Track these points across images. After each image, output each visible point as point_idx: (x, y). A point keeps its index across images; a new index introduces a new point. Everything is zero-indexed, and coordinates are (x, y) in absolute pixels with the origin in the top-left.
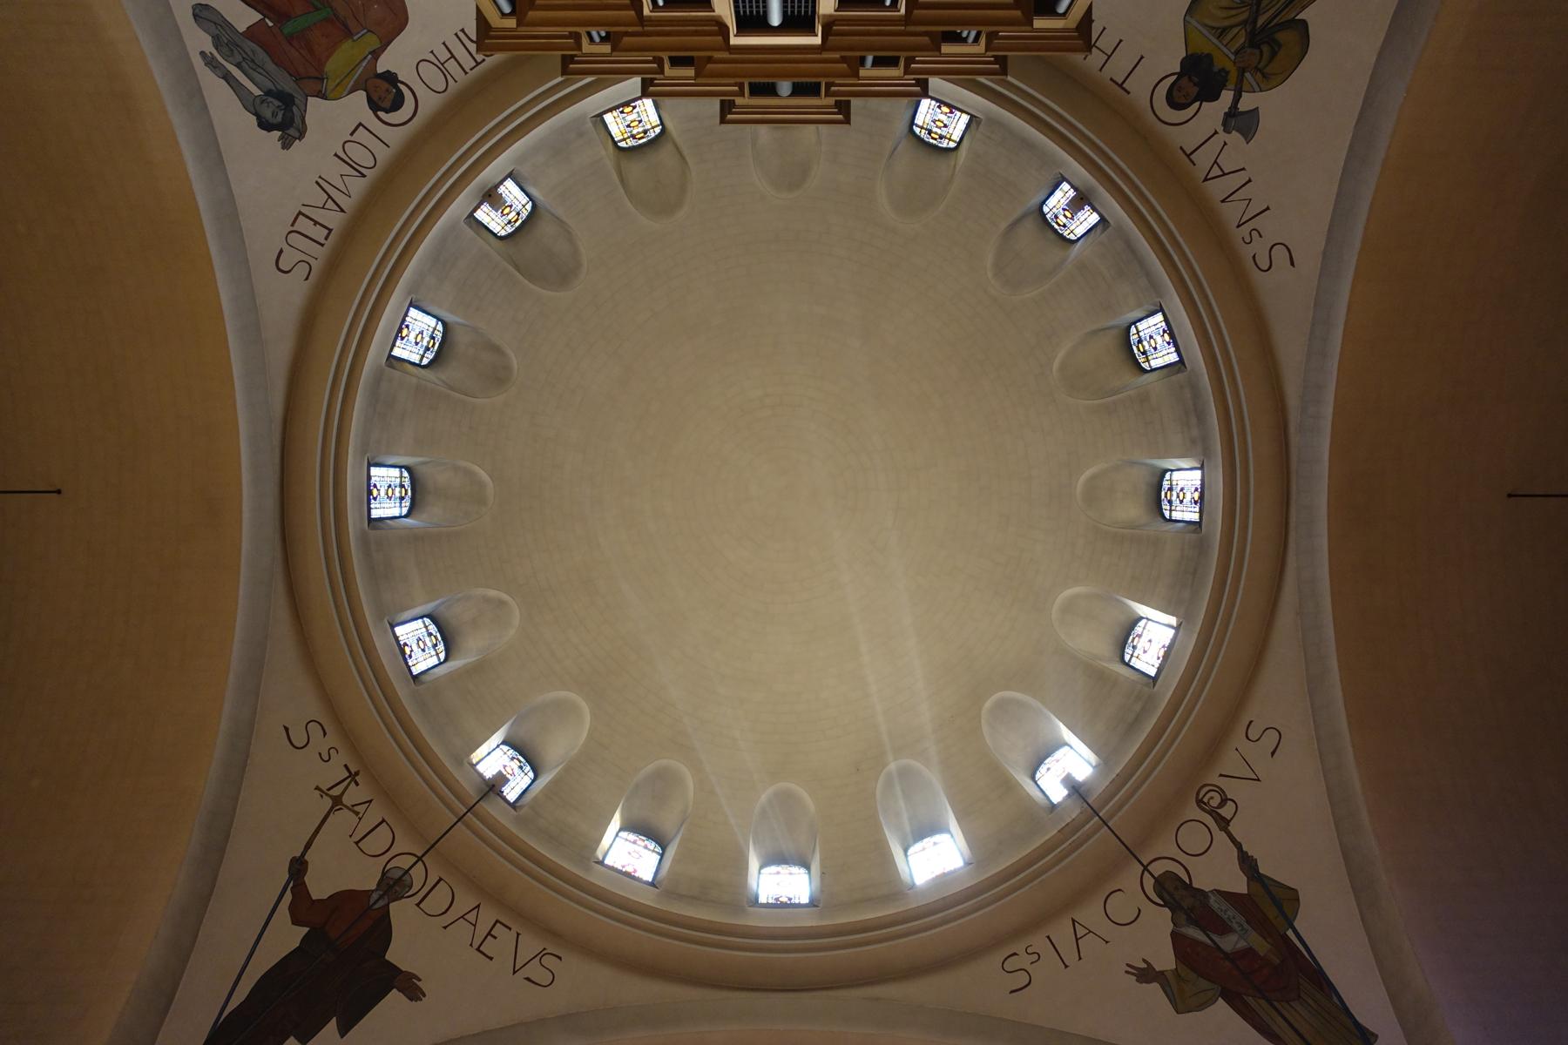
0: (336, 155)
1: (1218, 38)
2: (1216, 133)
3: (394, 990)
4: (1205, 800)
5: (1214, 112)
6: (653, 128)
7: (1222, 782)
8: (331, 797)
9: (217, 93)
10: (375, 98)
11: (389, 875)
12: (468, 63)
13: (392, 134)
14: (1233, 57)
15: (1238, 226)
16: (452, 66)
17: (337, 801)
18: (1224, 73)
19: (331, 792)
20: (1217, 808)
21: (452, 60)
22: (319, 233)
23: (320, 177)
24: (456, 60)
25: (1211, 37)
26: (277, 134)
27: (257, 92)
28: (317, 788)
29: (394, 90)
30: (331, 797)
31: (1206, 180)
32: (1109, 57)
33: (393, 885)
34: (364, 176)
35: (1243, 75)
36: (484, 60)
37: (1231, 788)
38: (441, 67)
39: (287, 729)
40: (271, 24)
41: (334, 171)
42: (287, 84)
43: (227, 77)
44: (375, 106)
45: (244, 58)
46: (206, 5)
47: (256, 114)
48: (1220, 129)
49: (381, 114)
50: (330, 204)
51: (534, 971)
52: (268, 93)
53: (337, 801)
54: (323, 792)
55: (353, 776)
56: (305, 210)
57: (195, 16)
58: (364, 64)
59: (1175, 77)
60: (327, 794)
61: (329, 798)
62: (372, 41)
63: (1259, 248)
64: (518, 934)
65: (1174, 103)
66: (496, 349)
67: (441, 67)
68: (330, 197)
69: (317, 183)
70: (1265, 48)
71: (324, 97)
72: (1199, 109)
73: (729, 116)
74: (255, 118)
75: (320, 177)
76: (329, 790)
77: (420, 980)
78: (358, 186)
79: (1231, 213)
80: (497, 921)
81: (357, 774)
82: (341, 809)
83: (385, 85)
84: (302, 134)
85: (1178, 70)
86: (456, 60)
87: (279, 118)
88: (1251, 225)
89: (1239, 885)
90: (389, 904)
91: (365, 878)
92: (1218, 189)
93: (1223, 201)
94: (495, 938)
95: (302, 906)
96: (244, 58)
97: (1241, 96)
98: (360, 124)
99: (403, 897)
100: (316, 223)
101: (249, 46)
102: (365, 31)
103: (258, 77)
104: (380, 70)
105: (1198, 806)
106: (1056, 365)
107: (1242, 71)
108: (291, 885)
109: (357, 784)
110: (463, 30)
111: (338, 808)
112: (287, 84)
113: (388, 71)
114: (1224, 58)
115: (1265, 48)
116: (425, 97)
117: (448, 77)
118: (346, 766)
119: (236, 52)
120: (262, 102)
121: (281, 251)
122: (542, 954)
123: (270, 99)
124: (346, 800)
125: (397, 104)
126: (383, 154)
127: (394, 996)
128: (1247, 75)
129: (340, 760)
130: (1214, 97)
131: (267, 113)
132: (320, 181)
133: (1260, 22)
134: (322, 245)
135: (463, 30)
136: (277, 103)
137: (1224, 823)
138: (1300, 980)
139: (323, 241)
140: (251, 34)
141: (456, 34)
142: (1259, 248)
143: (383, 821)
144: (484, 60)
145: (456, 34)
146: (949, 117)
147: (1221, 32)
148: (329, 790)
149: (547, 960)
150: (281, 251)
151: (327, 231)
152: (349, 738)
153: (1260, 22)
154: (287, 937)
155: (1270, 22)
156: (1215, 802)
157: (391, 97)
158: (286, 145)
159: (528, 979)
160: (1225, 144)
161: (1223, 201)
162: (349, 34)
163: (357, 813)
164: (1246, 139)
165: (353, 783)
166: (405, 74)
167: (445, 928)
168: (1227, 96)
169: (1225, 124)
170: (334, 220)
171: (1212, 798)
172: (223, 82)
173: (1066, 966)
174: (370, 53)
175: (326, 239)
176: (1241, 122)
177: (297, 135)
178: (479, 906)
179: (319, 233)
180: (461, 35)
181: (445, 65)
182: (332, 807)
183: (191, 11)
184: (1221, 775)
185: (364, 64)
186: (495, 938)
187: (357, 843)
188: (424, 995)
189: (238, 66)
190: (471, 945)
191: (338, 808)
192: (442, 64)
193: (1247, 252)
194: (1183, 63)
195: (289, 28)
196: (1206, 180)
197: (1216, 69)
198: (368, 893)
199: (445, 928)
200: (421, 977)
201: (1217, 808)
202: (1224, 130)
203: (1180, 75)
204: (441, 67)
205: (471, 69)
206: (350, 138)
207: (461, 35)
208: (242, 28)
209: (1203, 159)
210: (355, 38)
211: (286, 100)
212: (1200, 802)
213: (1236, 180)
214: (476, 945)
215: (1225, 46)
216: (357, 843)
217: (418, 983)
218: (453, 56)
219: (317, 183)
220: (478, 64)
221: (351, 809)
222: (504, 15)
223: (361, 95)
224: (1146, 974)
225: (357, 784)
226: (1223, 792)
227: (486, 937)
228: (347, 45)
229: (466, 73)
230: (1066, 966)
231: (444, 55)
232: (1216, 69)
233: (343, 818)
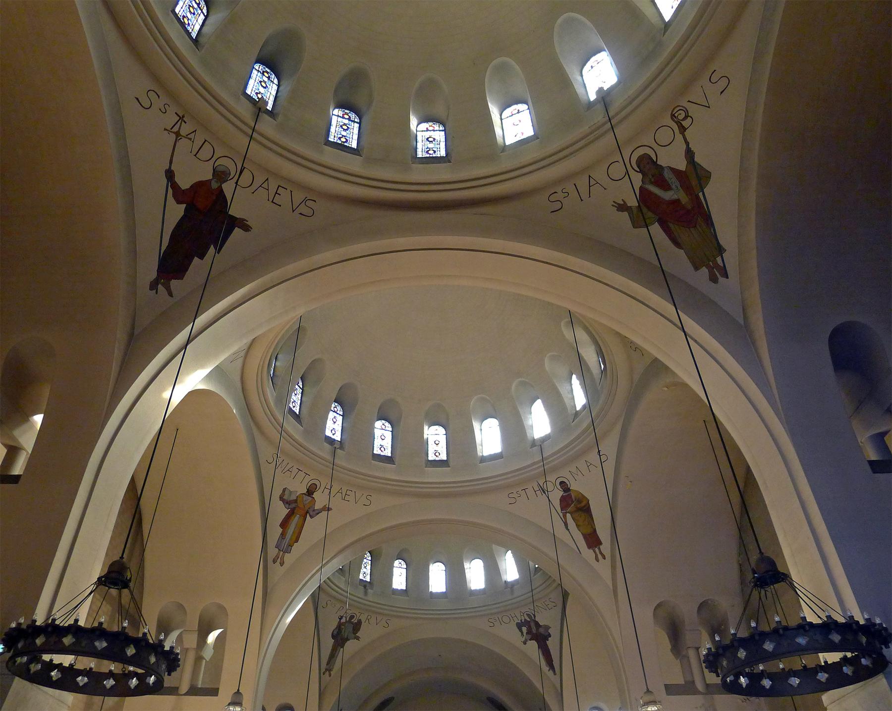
3: (236, 228)
4: (676, 115)
7: (689, 106)
8: (173, 132)
11: (217, 169)
17: (178, 134)
19: (173, 130)
20: (681, 120)
28: (165, 129)
30: (173, 132)
33: (221, 175)
37: (692, 109)
39: (137, 99)
51: (303, 209)
53: (178, 134)
54: (169, 131)
55: (181, 118)
60: (171, 132)
61: (173, 134)
64: (291, 191)
76: (171, 129)
77: (247, 221)
80: (279, 186)
81: (183, 116)
82: (181, 138)
89: (682, 165)
90: (221, 185)
91: (206, 174)
94: (280, 195)
95: (179, 195)
99: (227, 180)
105: (672, 118)
108: (170, 184)
109: (185, 123)
111: (180, 138)
118: (176, 113)
122: (305, 200)
124: (183, 133)
127: (237, 231)
129: (172, 109)
137: (683, 129)
138: (699, 218)
143: (205, 141)
148: (171, 129)
149: (310, 203)
152: (174, 96)
154: (177, 211)
156: (681, 117)
159: (301, 214)
163: (190, 139)
165: (183, 122)
167: (253, 193)
171: (680, 114)
173: (582, 200)
178: (267, 179)
182: (176, 139)
184: (689, 101)
186: (280, 195)
187: (195, 155)
188: (252, 229)
190: (268, 200)
191: (180, 138)
198: (210, 181)
199: (253, 193)
200: (247, 219)
201: (681, 120)
212: (673, 116)
214: (271, 200)
216: (195, 155)
217: (247, 223)
221: (187, 137)
224: (622, 207)
225: (185, 123)
226: (688, 112)
227: (275, 195)
230: (582, 200)
233: (183, 143)
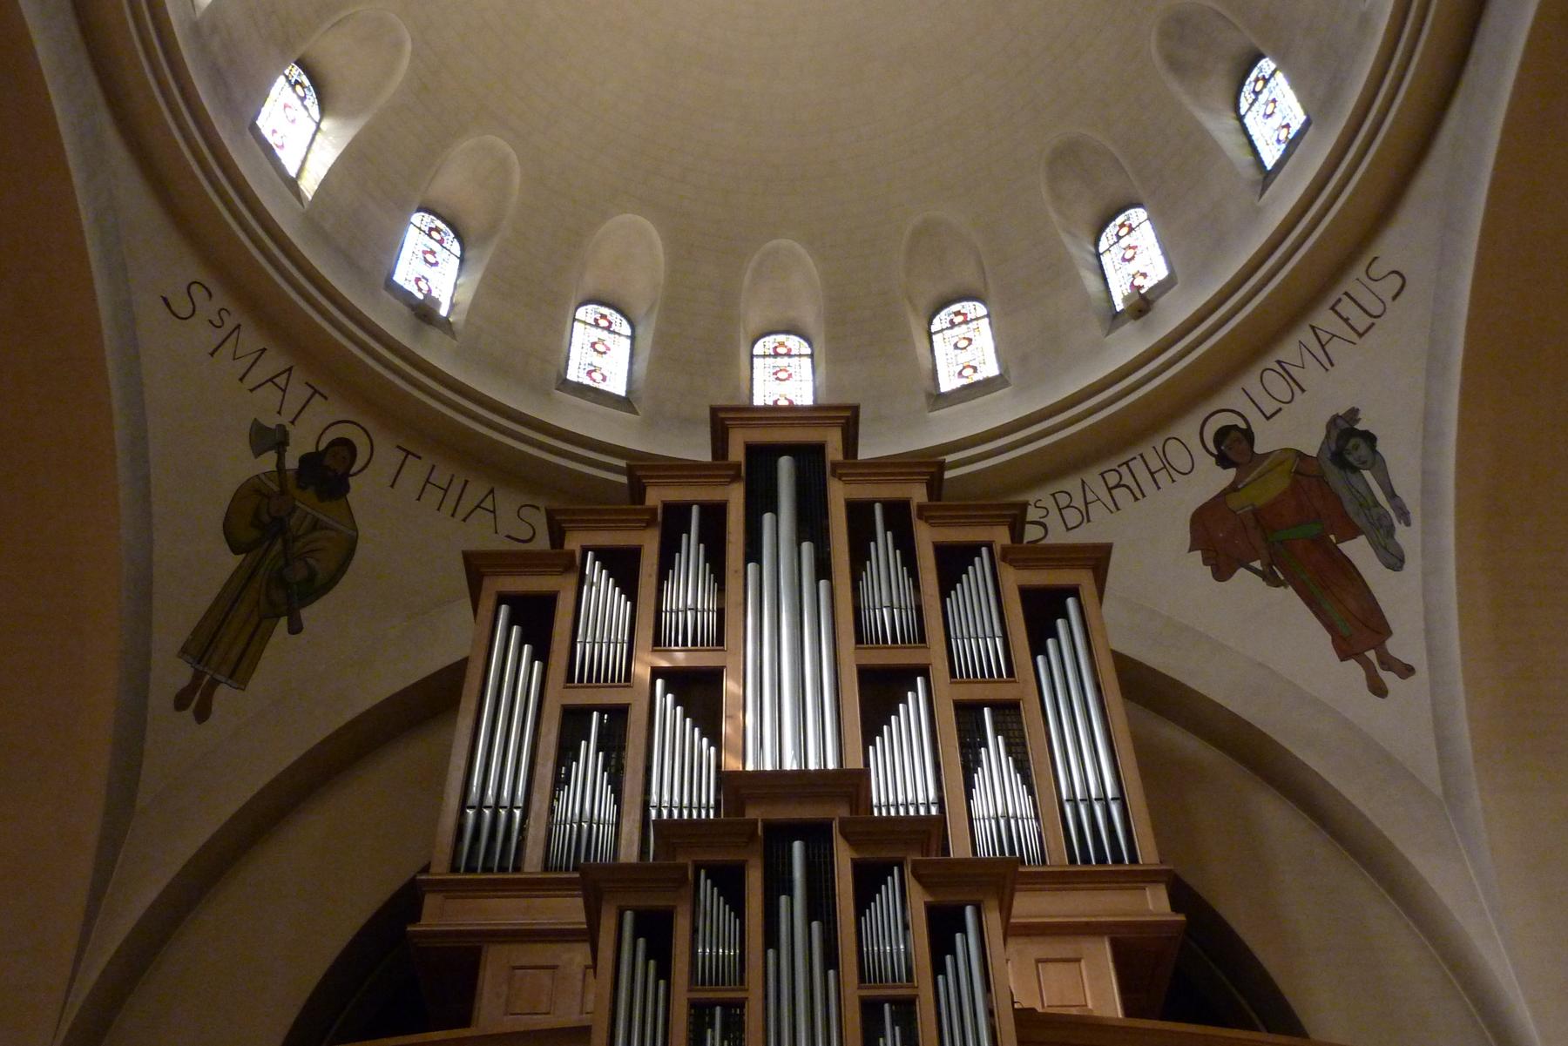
0: (1303, 390)
1: (318, 519)
2: (293, 422)
6: (942, 330)
9: (1406, 482)
10: (1245, 444)
12: (1137, 466)
14: (297, 503)
15: (238, 327)
16: (1155, 464)
18: (302, 487)
21: (1153, 470)
22: (1347, 308)
23: (1327, 370)
24: (1149, 470)
25: (325, 519)
26: (1359, 427)
27: (1367, 474)
29: (1223, 448)
31: (290, 370)
32: (427, 481)
34: (1279, 362)
35: (281, 485)
36: (1119, 466)
38: (1167, 466)
40: (1332, 537)
41: (1310, 375)
42: (1334, 476)
43: (1392, 495)
44: (1248, 435)
45: (1369, 510)
46: (1388, 568)
47: (1374, 451)
48: (289, 428)
49: (1243, 425)
50: (1324, 337)
52: (1355, 470)
56: (1354, 337)
57: (1402, 560)
58: (1248, 480)
59: (352, 471)
62: (1234, 502)
63: (207, 308)
65: (346, 445)
66: (1176, 66)
67: (1167, 465)
68: (1323, 346)
69: (1332, 365)
70: (266, 518)
71: (1300, 455)
72: (318, 443)
73: (848, 414)
74: (1377, 448)
75: (1327, 370)
78: (1288, 351)
79: (251, 340)
83: (1232, 455)
84: (1334, 421)
85: (352, 481)
86: (1149, 470)
87: (1353, 442)
92: (274, 362)
93: (265, 349)
96: (1369, 510)
97: (277, 466)
98: (1268, 418)
100: (1346, 320)
101: (1360, 521)
102: (1238, 513)
103: (1362, 489)
104: (1232, 472)
106: (408, 47)
107: (283, 492)
110: (1136, 499)
112: (1334, 476)
113: (1225, 467)
114: (306, 503)
115: (266, 518)
117: (1161, 454)
119: (1375, 518)
120: (1364, 463)
121: (1394, 298)
123: (1356, 463)
125: (1222, 434)
126: (1251, 381)
128: (276, 489)
130: (305, 460)
131: (1364, 450)
132: (1328, 365)
133: (278, 546)
134: (1346, 294)
135: (1136, 499)
136: (1351, 459)
139: (1345, 298)
140: (1353, 532)
141: (1144, 496)
142: (207, 308)
144: (1119, 466)
145: (1144, 496)
146: (591, 365)
147: (316, 525)
150: (1394, 298)
151: (1337, 308)
153: (278, 546)
155: (270, 545)
157: (1227, 442)
158: (1353, 414)
160: (279, 413)
161: (265, 349)
162: (1257, 513)
164: (259, 423)
166: (1207, 463)
168: (292, 462)
170: (1324, 319)
172: (1398, 492)
174: (1239, 490)
175: (1339, 300)
176: (268, 439)
177: (1339, 421)
179: (1347, 308)
180: (1139, 495)
181: (1162, 466)
183: (1405, 566)
185: (1248, 480)
189: (1377, 504)
192: (1165, 467)
193: (221, 299)
194: (347, 488)
196: (290, 370)
202: (284, 426)
203: (347, 475)
204: (1166, 463)
205: (1135, 458)
206: (1282, 405)
207: (1139, 495)
208: (1362, 539)
209: (298, 393)
210: (1250, 508)
211: (1339, 457)
213: (259, 374)
215: (308, 513)
218: (1152, 474)
219: (1332, 365)
220: (1126, 463)
222: (1074, 591)
223: (1259, 448)
228: (1259, 502)
229: (1142, 456)
231: (1162, 477)
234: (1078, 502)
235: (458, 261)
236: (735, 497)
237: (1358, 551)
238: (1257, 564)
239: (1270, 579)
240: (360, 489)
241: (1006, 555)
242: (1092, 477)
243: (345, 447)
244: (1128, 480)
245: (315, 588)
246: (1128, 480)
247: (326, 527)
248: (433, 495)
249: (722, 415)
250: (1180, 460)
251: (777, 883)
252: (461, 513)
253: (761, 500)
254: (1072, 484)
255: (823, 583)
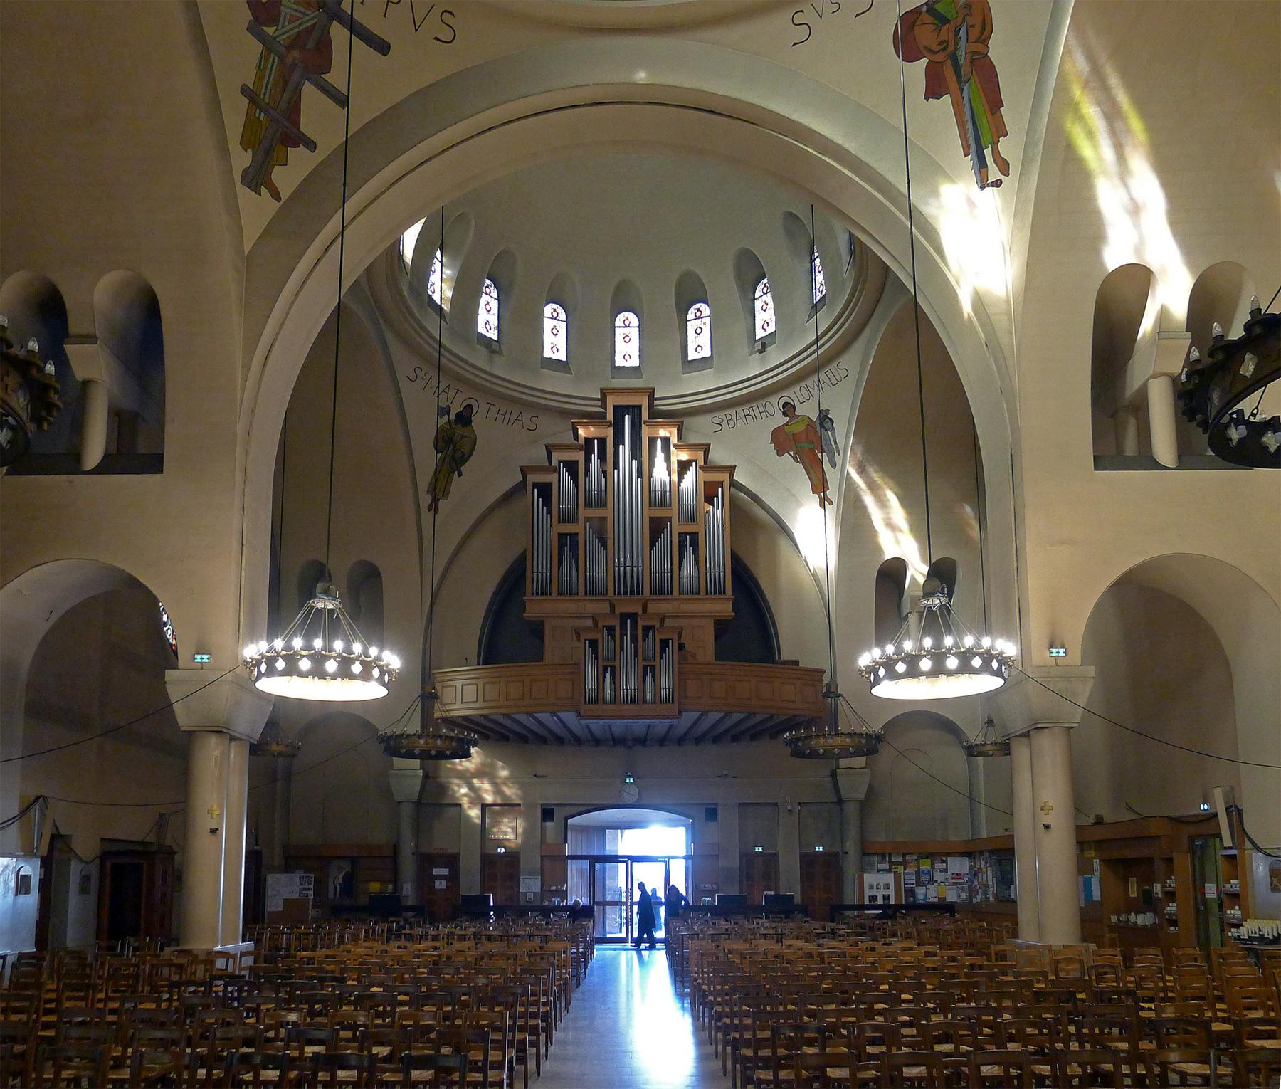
5: (454, 411)
13: (791, 395)
27: (829, 432)
43: (836, 443)
44: (794, 407)
67: (766, 410)
85: (472, 418)
88: (427, 380)
114: (459, 430)
116: (775, 402)
125: (785, 405)
130: (457, 415)
131: (829, 424)
147: (463, 437)
162: (793, 435)
168: (452, 417)
169: (450, 407)
189: (831, 444)
195: (811, 446)
197: (460, 425)
203: (471, 417)
222: (721, 484)
232: (460, 425)
234: (734, 419)
235: (497, 301)
236: (609, 433)
237: (824, 458)
238: (792, 453)
239: (795, 458)
240: (476, 420)
241: (700, 467)
242: (739, 410)
243: (470, 407)
244: (752, 413)
245: (464, 459)
246: (752, 413)
247: (466, 437)
248: (500, 418)
249: (604, 391)
250: (771, 411)
251: (623, 634)
252: (510, 423)
253: (619, 439)
254: (732, 411)
255: (639, 479)
